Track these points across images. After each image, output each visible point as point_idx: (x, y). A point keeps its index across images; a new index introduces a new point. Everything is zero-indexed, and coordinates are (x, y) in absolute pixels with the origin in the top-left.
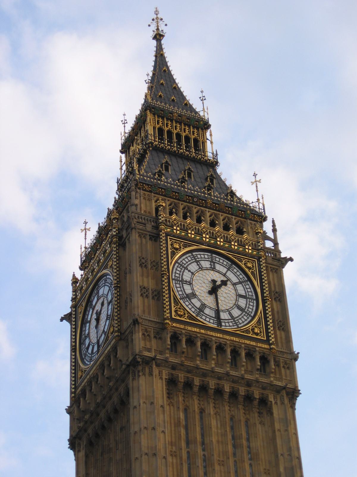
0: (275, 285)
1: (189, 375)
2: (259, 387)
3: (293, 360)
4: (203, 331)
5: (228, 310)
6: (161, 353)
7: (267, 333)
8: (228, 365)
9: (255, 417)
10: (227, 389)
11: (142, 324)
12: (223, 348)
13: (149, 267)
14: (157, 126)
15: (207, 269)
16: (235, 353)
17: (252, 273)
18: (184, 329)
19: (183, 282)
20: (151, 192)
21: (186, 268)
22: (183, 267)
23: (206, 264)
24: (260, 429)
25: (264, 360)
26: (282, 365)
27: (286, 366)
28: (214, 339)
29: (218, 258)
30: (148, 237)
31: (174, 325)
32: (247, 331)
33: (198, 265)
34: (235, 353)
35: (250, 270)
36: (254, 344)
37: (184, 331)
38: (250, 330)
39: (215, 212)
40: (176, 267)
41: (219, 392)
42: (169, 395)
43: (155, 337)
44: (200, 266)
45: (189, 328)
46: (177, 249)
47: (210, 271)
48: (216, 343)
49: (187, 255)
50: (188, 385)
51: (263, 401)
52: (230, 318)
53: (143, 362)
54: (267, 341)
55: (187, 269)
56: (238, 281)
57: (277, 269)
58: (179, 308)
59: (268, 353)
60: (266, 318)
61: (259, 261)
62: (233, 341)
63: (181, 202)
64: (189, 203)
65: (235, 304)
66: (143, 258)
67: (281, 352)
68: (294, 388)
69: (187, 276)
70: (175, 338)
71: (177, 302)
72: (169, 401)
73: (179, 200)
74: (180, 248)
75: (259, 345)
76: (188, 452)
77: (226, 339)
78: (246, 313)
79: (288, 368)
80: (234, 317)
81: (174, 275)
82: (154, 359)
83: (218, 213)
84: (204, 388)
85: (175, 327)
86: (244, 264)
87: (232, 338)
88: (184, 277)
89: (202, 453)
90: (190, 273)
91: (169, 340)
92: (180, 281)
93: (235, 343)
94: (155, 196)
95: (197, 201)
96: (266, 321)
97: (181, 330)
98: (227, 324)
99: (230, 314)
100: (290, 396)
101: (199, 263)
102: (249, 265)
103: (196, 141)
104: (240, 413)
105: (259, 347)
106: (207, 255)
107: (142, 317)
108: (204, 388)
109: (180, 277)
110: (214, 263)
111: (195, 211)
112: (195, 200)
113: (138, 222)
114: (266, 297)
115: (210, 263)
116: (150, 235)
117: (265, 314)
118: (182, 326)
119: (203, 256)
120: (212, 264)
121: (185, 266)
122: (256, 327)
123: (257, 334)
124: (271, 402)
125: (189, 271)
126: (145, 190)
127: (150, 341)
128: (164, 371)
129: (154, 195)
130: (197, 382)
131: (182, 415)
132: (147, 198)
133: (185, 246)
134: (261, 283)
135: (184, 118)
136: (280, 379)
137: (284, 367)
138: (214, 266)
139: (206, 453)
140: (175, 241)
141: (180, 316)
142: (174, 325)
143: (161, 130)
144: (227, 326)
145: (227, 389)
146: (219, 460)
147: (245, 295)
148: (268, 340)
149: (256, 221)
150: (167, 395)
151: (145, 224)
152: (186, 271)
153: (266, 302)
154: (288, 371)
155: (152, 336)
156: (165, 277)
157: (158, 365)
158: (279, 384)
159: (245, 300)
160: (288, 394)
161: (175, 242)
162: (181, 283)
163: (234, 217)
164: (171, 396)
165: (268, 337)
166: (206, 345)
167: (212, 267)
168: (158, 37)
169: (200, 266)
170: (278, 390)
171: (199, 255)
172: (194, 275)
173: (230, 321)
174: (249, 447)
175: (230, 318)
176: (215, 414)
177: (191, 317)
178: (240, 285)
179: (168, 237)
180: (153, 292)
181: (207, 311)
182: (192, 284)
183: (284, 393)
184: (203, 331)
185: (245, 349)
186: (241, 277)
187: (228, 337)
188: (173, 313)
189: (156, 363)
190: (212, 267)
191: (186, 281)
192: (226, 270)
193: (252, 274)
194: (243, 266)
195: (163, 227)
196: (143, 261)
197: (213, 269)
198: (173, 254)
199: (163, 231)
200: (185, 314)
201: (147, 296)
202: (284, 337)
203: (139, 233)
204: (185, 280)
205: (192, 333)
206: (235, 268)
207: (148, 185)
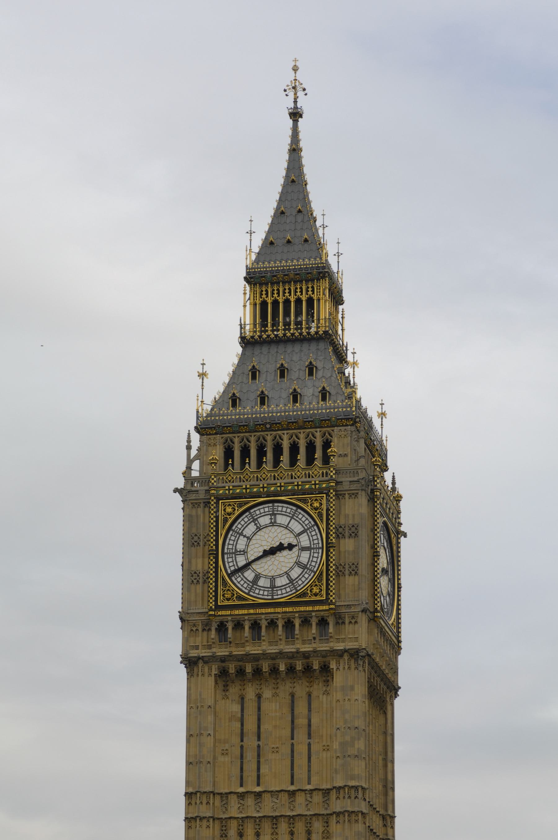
0: (354, 516)
1: (241, 663)
2: (318, 656)
3: (360, 613)
4: (252, 611)
5: (286, 572)
6: (210, 647)
7: (327, 589)
8: (283, 642)
9: (317, 689)
10: (282, 668)
11: (188, 620)
12: (276, 623)
13: (201, 544)
14: (258, 302)
15: (266, 526)
16: (289, 625)
17: (320, 515)
18: (230, 615)
19: (237, 552)
20: (216, 434)
21: (241, 534)
22: (238, 533)
23: (264, 521)
24: (325, 699)
25: (323, 622)
26: (347, 621)
27: (353, 621)
28: (263, 616)
29: (279, 507)
30: (202, 505)
31: (220, 613)
32: (304, 594)
33: (256, 524)
34: (289, 625)
35: (316, 510)
36: (310, 608)
37: (230, 618)
38: (309, 592)
39: (295, 431)
40: (229, 536)
41: (274, 670)
42: (226, 688)
43: (204, 630)
44: (258, 525)
45: (237, 612)
46: (229, 514)
47: (270, 528)
48: (267, 620)
49: (244, 516)
50: (241, 672)
51: (325, 669)
52: (288, 582)
53: (190, 663)
54: (326, 602)
55: (242, 535)
56: (303, 529)
57: (357, 493)
58: (228, 590)
59: (327, 615)
60: (328, 570)
61: (328, 495)
62: (286, 612)
63: (253, 434)
64: (262, 431)
65: (296, 562)
66: (196, 535)
67: (348, 605)
68: (358, 647)
69: (242, 543)
70: (222, 628)
71: (225, 583)
72: (224, 694)
73: (249, 432)
74: (235, 509)
75: (317, 608)
76: (242, 747)
77: (278, 613)
78: (308, 569)
79: (356, 622)
80: (292, 579)
81: (226, 547)
82: (199, 658)
83: (299, 431)
84: (258, 672)
85: (222, 615)
86: (311, 505)
87: (285, 609)
88: (238, 547)
89: (256, 743)
90: (246, 539)
91: (213, 632)
92: (232, 553)
93: (287, 615)
94: (222, 438)
95: (270, 428)
96: (328, 575)
97: (227, 617)
98: (284, 591)
99: (289, 577)
100: (356, 656)
101: (256, 522)
102: (316, 504)
103: (310, 301)
104: (301, 689)
105: (317, 611)
106: (266, 508)
107: (190, 611)
108: (258, 672)
109: (234, 548)
110: (275, 515)
111: (269, 438)
112: (268, 426)
113: (189, 492)
114: (330, 543)
115: (270, 517)
116: (204, 502)
117: (328, 565)
118: (228, 613)
119: (262, 511)
120: (273, 517)
121: (240, 532)
122: (316, 585)
123: (316, 595)
124: (333, 669)
125: (245, 536)
126: (210, 434)
127: (199, 636)
128: (213, 666)
129: (221, 436)
130: (249, 669)
131: (236, 708)
132: (212, 444)
133: (240, 506)
134: (328, 524)
135: (292, 276)
136: (344, 640)
137: (350, 622)
138: (275, 519)
139: (260, 743)
140: (228, 503)
141: (228, 599)
142: (220, 613)
143: (264, 304)
144: (281, 596)
145: (282, 668)
146: (273, 748)
147: (309, 545)
148: (327, 599)
149: (347, 425)
150: (223, 688)
151: (197, 491)
152: (241, 537)
153: (330, 550)
154: (356, 626)
155: (200, 630)
156: (212, 558)
157: (206, 662)
158: (340, 646)
159: (309, 552)
160: (352, 656)
161: (230, 505)
162: (234, 555)
163: (318, 430)
164: (228, 688)
165: (327, 594)
166: (255, 626)
167: (273, 521)
168: (296, 115)
169: (258, 525)
170: (340, 654)
171: (256, 511)
172: (250, 540)
173: (287, 586)
174: (309, 725)
175: (288, 582)
176: (273, 696)
177: (240, 598)
178: (305, 534)
179: (221, 501)
180: (205, 575)
181: (262, 582)
182: (247, 552)
183: (346, 657)
184: (252, 611)
185: (300, 618)
186: (307, 522)
187: (279, 610)
188: (220, 598)
189: (203, 660)
190: (273, 521)
191: (240, 551)
192: (289, 519)
193: (319, 516)
194: (308, 509)
195: (213, 492)
196: (196, 538)
197: (273, 524)
198: (225, 520)
199: (213, 498)
200: (234, 595)
201: (198, 581)
202: (357, 583)
203: (192, 503)
204: (239, 550)
205: (239, 617)
206: (300, 513)
207: (211, 428)
